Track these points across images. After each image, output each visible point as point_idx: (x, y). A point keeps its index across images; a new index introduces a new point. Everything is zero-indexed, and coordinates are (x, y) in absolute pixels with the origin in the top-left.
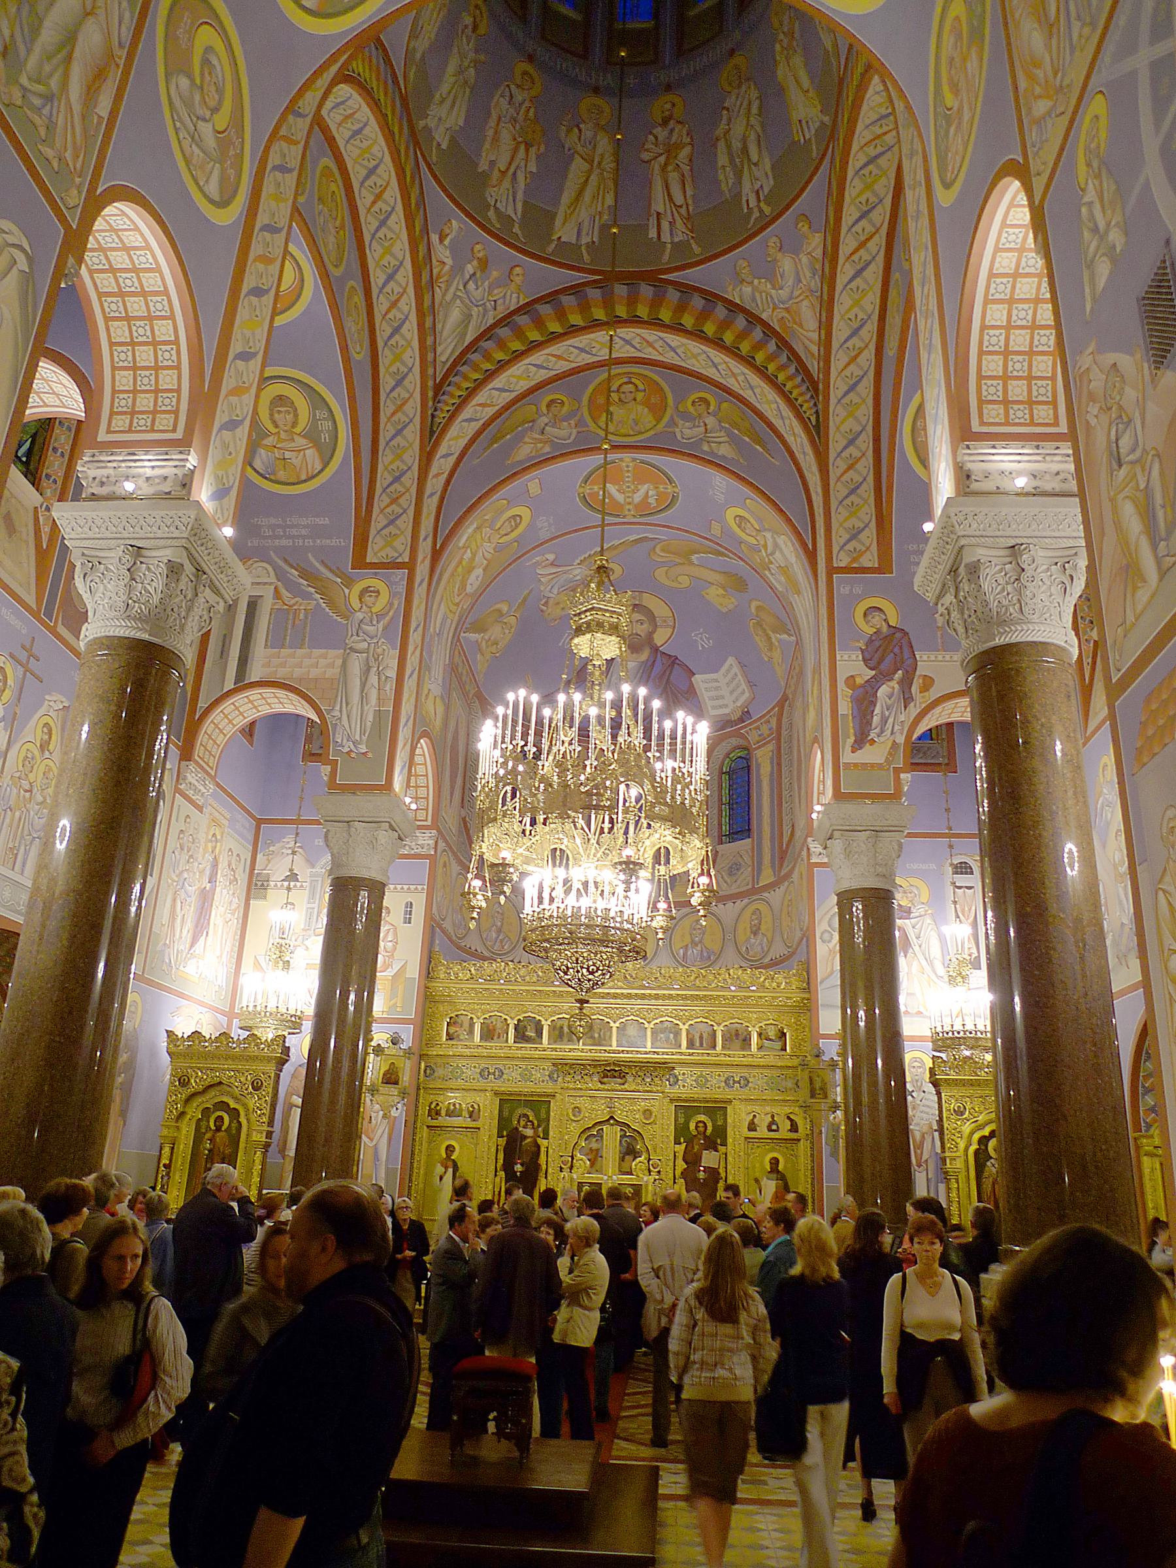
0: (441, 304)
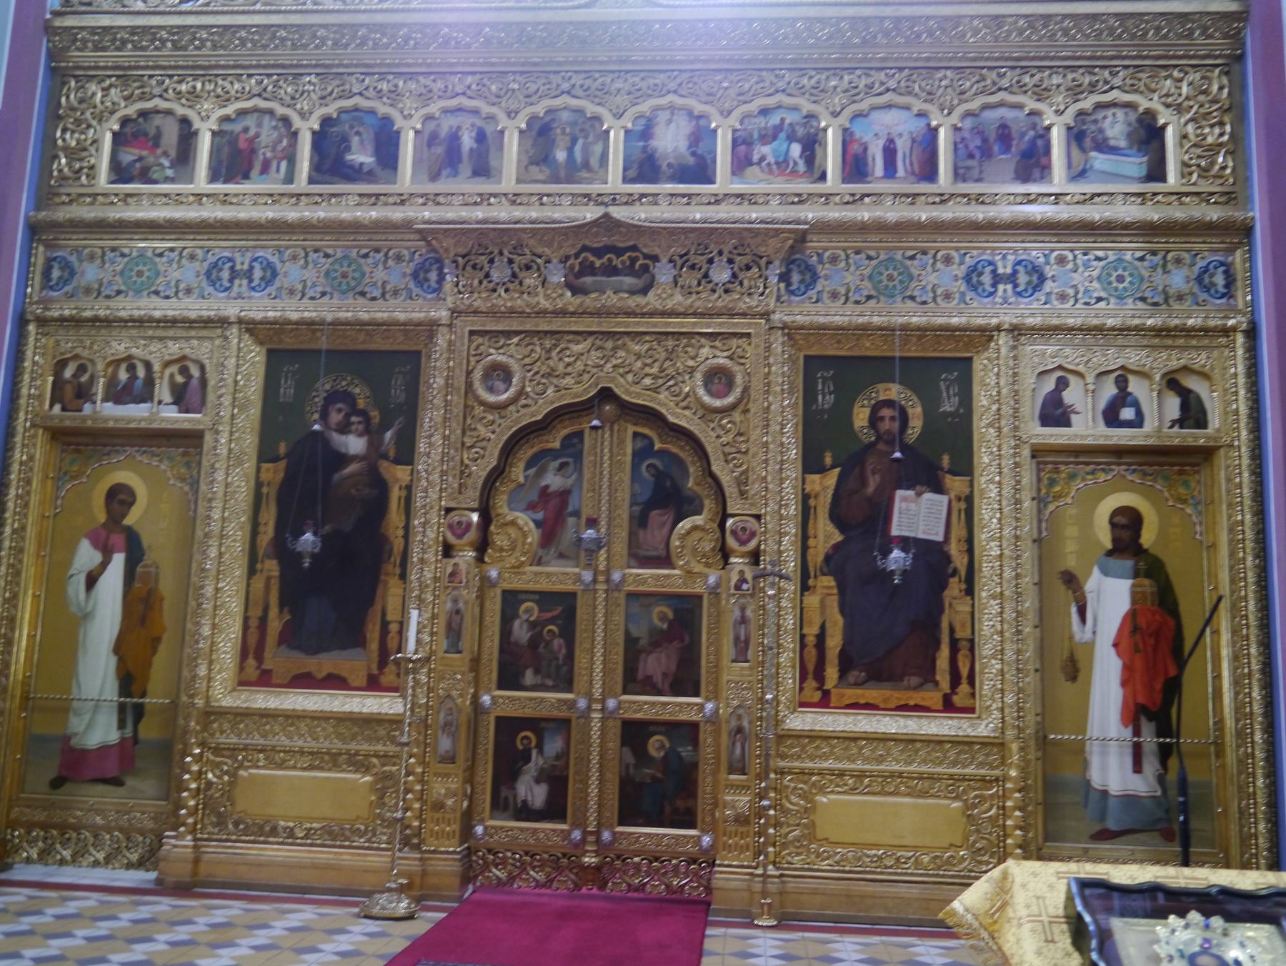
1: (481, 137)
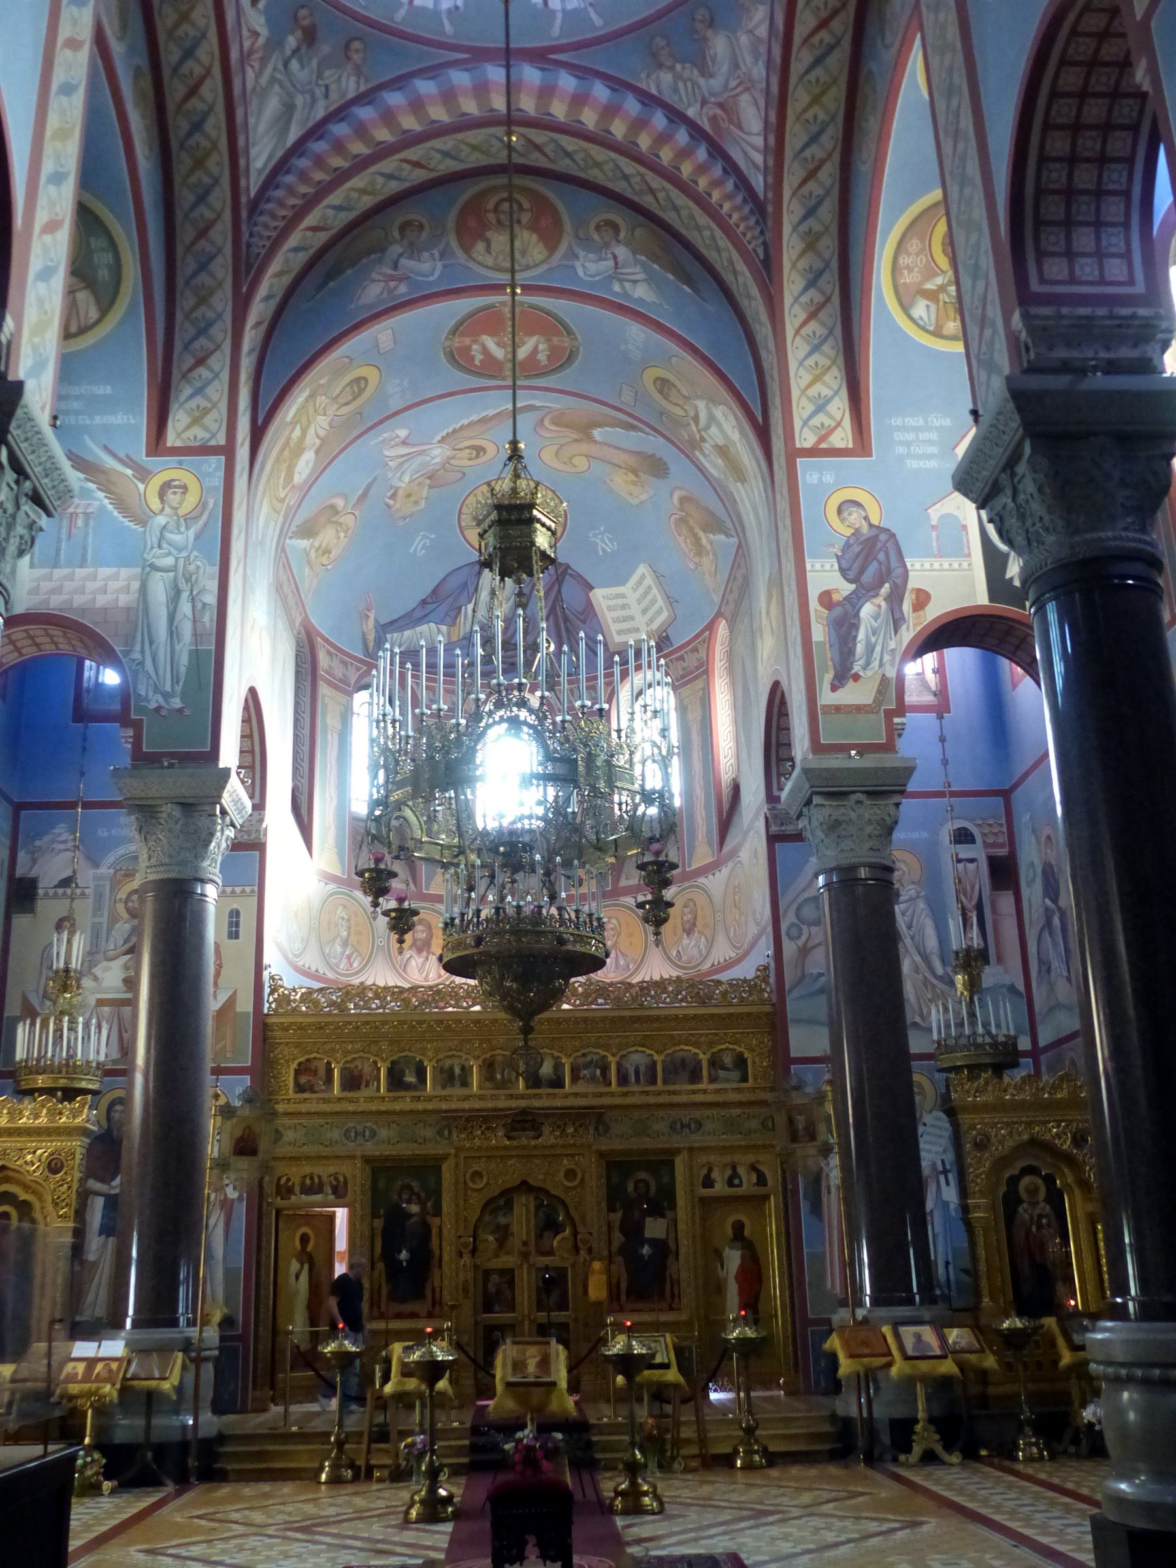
0: (254, 89)
1: (463, 1068)
